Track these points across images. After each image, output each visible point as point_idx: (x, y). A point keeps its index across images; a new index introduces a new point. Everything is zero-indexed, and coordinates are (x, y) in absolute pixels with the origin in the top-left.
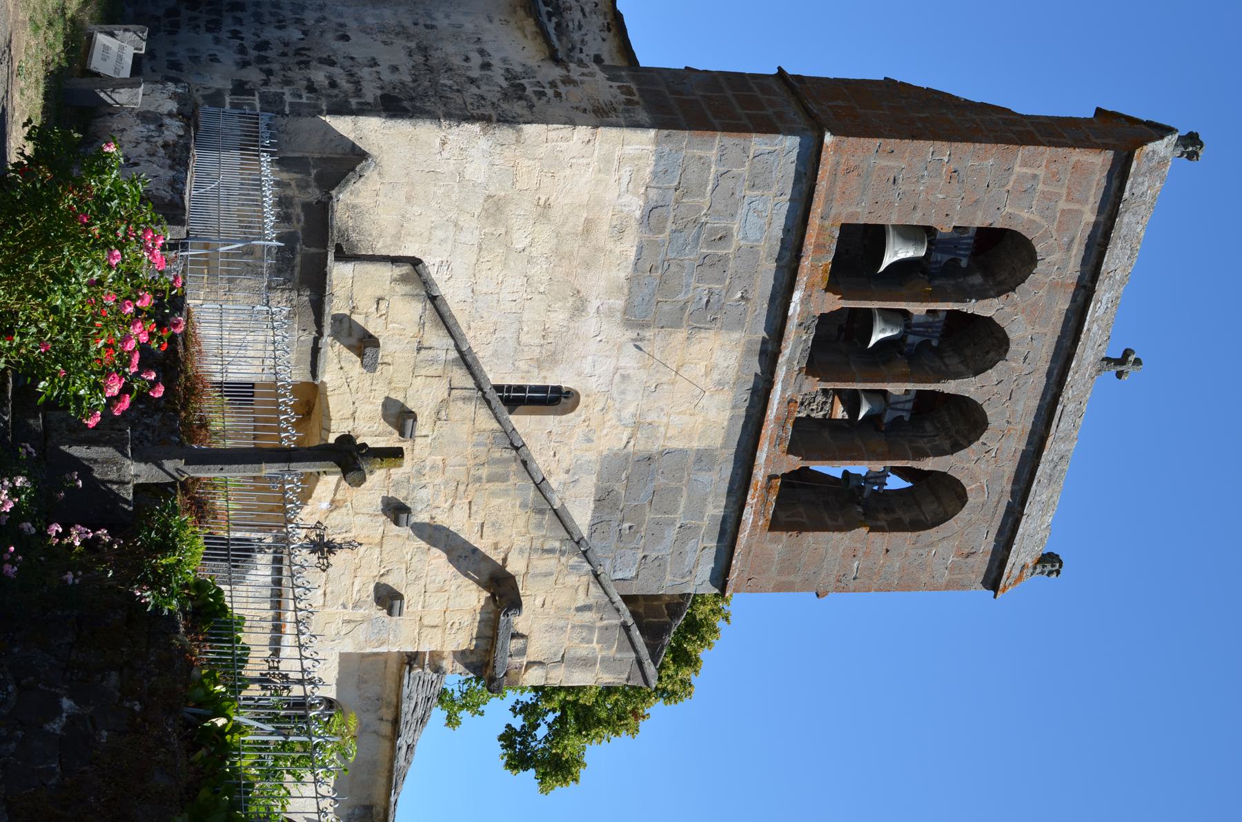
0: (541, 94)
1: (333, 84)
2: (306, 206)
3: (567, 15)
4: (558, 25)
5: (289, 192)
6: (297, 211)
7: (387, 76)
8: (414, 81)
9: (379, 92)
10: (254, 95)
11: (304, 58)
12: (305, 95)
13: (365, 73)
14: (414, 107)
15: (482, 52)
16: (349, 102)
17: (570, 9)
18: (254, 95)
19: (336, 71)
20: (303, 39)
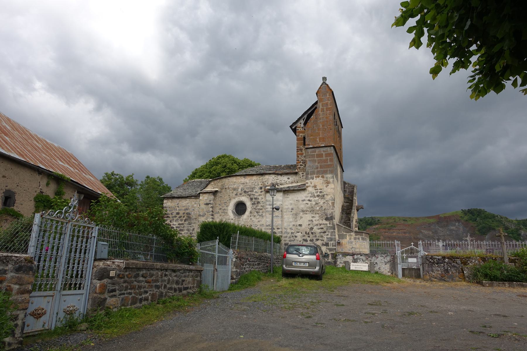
0: (320, 192)
1: (322, 228)
2: (356, 235)
3: (278, 182)
4: (281, 185)
5: (353, 238)
6: (357, 236)
7: (317, 218)
8: (318, 214)
9: (324, 221)
10: (328, 243)
11: (310, 233)
12: (327, 233)
13: (315, 223)
14: (330, 215)
15: (303, 201)
16: (329, 226)
17: (276, 182)
18: (328, 243)
19: (315, 228)
20: (301, 233)
